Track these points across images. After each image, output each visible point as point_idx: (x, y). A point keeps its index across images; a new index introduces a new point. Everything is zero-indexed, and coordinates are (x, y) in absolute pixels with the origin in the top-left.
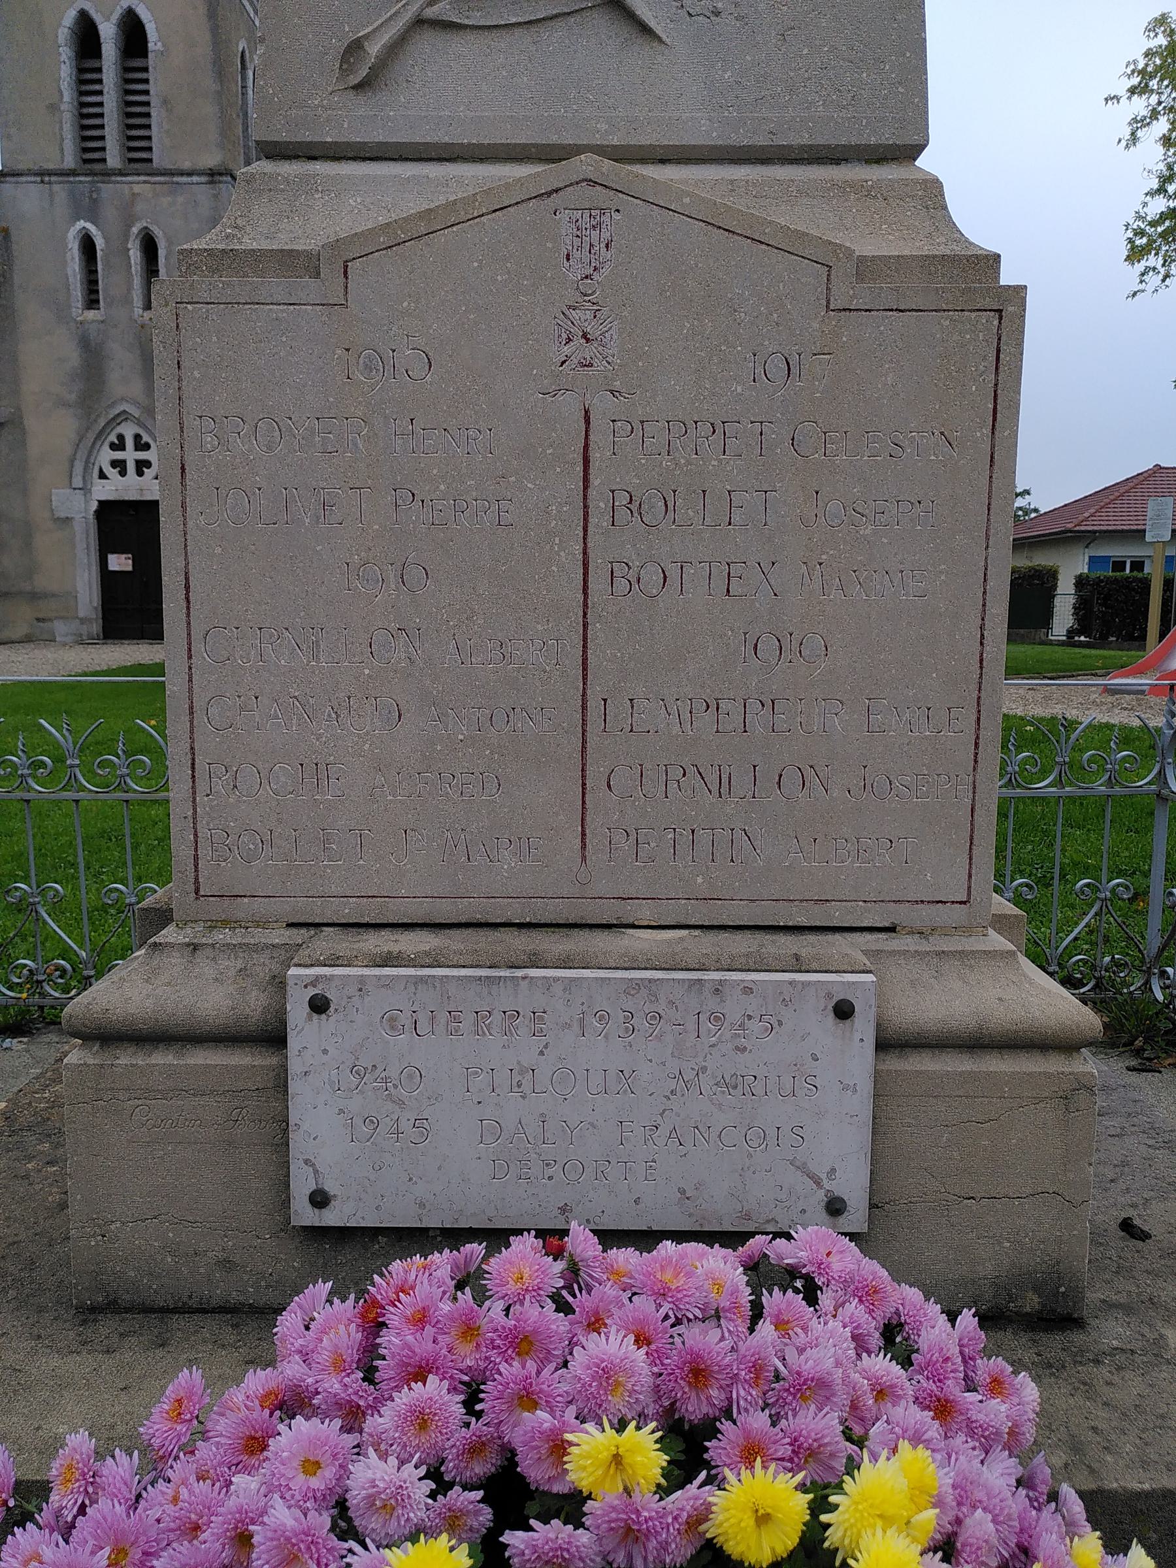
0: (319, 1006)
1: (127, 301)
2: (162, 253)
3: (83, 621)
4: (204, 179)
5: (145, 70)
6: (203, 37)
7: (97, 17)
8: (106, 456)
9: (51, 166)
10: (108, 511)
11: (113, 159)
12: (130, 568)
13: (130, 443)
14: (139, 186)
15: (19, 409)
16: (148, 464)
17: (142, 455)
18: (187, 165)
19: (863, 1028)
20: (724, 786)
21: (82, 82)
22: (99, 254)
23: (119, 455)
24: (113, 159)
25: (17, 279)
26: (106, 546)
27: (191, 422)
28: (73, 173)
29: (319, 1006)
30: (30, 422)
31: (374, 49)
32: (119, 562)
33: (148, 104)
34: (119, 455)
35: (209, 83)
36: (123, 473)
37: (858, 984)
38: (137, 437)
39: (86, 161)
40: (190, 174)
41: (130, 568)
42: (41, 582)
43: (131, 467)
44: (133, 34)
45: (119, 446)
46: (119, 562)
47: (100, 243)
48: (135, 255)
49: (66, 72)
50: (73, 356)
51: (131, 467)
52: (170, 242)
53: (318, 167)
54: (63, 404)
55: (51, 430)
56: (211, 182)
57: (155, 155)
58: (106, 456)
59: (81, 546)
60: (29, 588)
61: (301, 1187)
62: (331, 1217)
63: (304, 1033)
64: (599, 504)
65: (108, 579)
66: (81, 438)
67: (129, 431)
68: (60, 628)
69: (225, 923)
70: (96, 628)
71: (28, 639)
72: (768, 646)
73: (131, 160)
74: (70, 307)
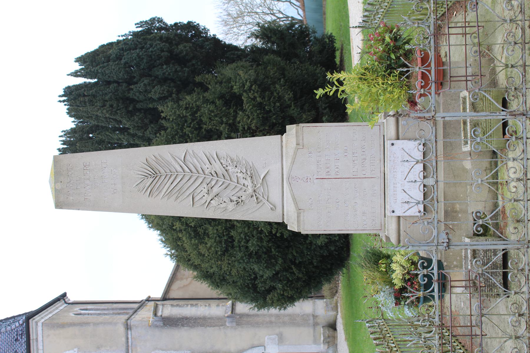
0: (393, 212)
4: (129, 332)
6: (71, 331)
18: (124, 339)
19: (395, 142)
20: (365, 159)
27: (319, 229)
29: (393, 212)
31: (272, 206)
40: (127, 338)
53: (285, 214)
56: (131, 329)
62: (422, 210)
63: (397, 213)
64: (327, 177)
69: (385, 227)
72: (346, 154)
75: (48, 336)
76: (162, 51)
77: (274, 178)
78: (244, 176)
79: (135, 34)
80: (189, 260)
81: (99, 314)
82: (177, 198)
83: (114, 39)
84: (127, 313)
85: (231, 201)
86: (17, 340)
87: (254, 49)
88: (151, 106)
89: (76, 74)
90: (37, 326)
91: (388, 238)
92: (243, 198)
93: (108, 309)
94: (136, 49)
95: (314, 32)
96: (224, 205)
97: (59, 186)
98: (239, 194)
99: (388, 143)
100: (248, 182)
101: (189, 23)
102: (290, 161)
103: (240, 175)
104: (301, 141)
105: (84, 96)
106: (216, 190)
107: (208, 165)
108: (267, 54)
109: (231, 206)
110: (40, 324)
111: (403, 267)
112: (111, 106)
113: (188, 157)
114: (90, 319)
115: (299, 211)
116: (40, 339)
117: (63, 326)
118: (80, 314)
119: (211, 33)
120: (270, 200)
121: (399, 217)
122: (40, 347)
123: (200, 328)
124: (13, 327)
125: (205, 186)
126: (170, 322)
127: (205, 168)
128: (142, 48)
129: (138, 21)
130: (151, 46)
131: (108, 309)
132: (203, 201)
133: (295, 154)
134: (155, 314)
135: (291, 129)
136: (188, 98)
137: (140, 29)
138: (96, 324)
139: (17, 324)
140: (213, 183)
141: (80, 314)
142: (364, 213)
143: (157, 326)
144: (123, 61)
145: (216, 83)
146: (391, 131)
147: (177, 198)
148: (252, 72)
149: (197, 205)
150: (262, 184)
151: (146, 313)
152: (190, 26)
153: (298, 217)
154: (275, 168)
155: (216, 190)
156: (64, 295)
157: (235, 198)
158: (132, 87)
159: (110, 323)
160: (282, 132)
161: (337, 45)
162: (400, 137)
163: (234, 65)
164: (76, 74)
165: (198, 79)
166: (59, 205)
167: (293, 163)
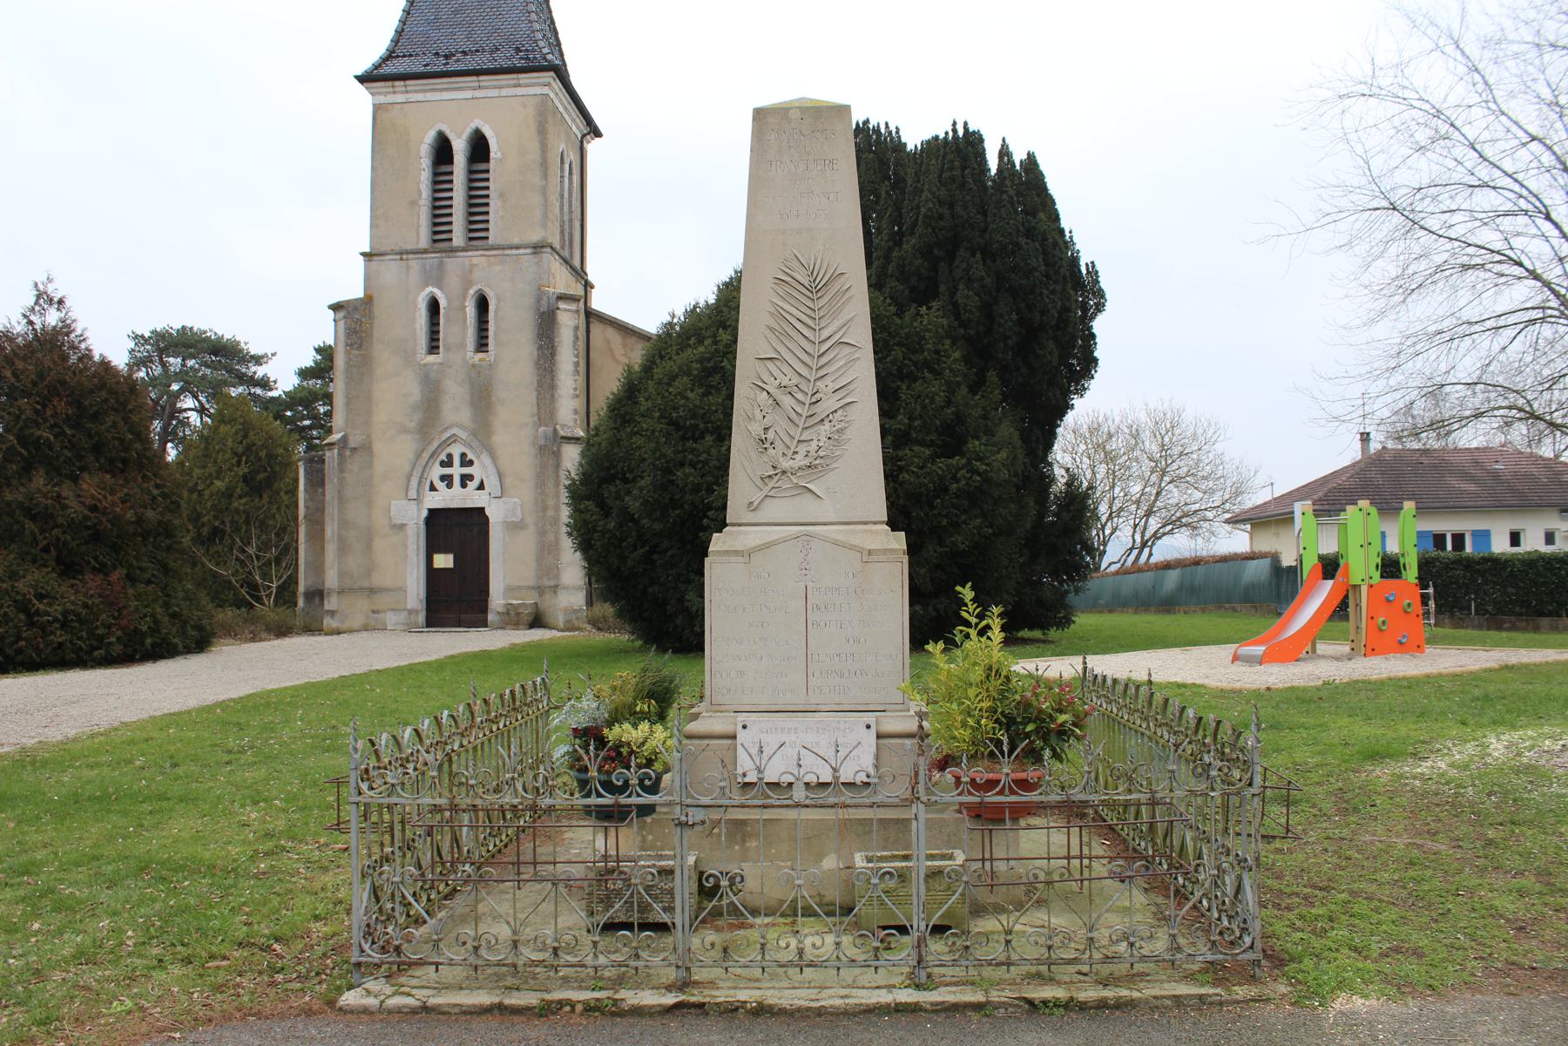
0: (744, 727)
1: (463, 345)
2: (492, 308)
3: (410, 612)
4: (529, 251)
5: (487, 171)
6: (533, 146)
7: (451, 136)
8: (437, 471)
9: (409, 248)
10: (435, 516)
11: (458, 238)
12: (451, 565)
13: (457, 461)
14: (477, 258)
15: (369, 436)
16: (470, 477)
17: (466, 470)
18: (516, 241)
19: (873, 730)
21: (435, 183)
22: (442, 311)
23: (447, 471)
24: (458, 238)
25: (376, 334)
26: (432, 548)
28: (425, 251)
29: (744, 727)
30: (379, 447)
32: (443, 561)
33: (487, 196)
34: (447, 471)
35: (536, 180)
36: (450, 486)
37: (872, 722)
38: (463, 455)
39: (435, 241)
40: (517, 248)
41: (451, 565)
42: (378, 580)
43: (457, 480)
44: (479, 148)
45: (448, 463)
46: (443, 561)
47: (443, 303)
48: (471, 311)
49: (425, 176)
50: (414, 391)
51: (457, 480)
52: (498, 299)
54: (405, 430)
55: (393, 451)
57: (491, 234)
58: (437, 471)
59: (412, 547)
60: (366, 584)
61: (740, 771)
62: (747, 780)
65: (433, 574)
66: (419, 456)
67: (456, 451)
68: (391, 619)
70: (421, 618)
71: (366, 628)
73: (471, 239)
74: (414, 353)
75: (525, 106)
76: (1042, 313)
77: (806, 508)
78: (813, 453)
79: (1075, 261)
80: (662, 357)
81: (562, 197)
82: (771, 329)
83: (1065, 223)
84: (563, 247)
85: (766, 429)
86: (518, 50)
87: (1047, 480)
88: (942, 288)
89: (1004, 153)
90: (543, 86)
91: (695, 717)
92: (771, 451)
93: (571, 212)
94: (1046, 265)
95: (1077, 591)
96: (759, 416)
97: (794, 115)
98: (778, 443)
99: (870, 718)
100: (800, 461)
101: (1095, 361)
102: (840, 537)
103: (814, 445)
104: (875, 558)
105: (963, 168)
106: (786, 400)
107: (833, 387)
108: (1037, 502)
109: (756, 429)
110: (546, 90)
111: (643, 744)
112: (941, 217)
113: (848, 350)
114: (554, 181)
115: (747, 554)
116: (520, 91)
117: (542, 131)
118: (562, 162)
119: (1076, 401)
120: (768, 501)
121: (734, 737)
122: (504, 92)
123: (535, 379)
124: (542, 44)
125: (794, 382)
126: (546, 324)
127: (828, 380)
128: (1047, 276)
129: (1098, 268)
130: (1053, 292)
131: (571, 212)
132: (766, 377)
133: (853, 548)
134: (561, 297)
135: (899, 541)
136: (957, 355)
137: (1084, 271)
138: (544, 191)
139: (546, 51)
140: (800, 396)
141: (562, 162)
142: (742, 673)
143: (539, 301)
144: (1022, 240)
145: (984, 409)
146: (893, 724)
147: (771, 329)
148: (1005, 474)
149: (760, 366)
150: (797, 486)
151: (562, 281)
152: (1089, 363)
153: (736, 553)
154: (826, 511)
155: (786, 400)
156: (598, 134)
157: (771, 435)
158: (978, 255)
159: (545, 215)
160: (894, 524)
161: (1053, 633)
162: (882, 741)
163: (1019, 443)
164: (1004, 153)
165: (992, 376)
166: (760, 115)
167: (836, 543)
